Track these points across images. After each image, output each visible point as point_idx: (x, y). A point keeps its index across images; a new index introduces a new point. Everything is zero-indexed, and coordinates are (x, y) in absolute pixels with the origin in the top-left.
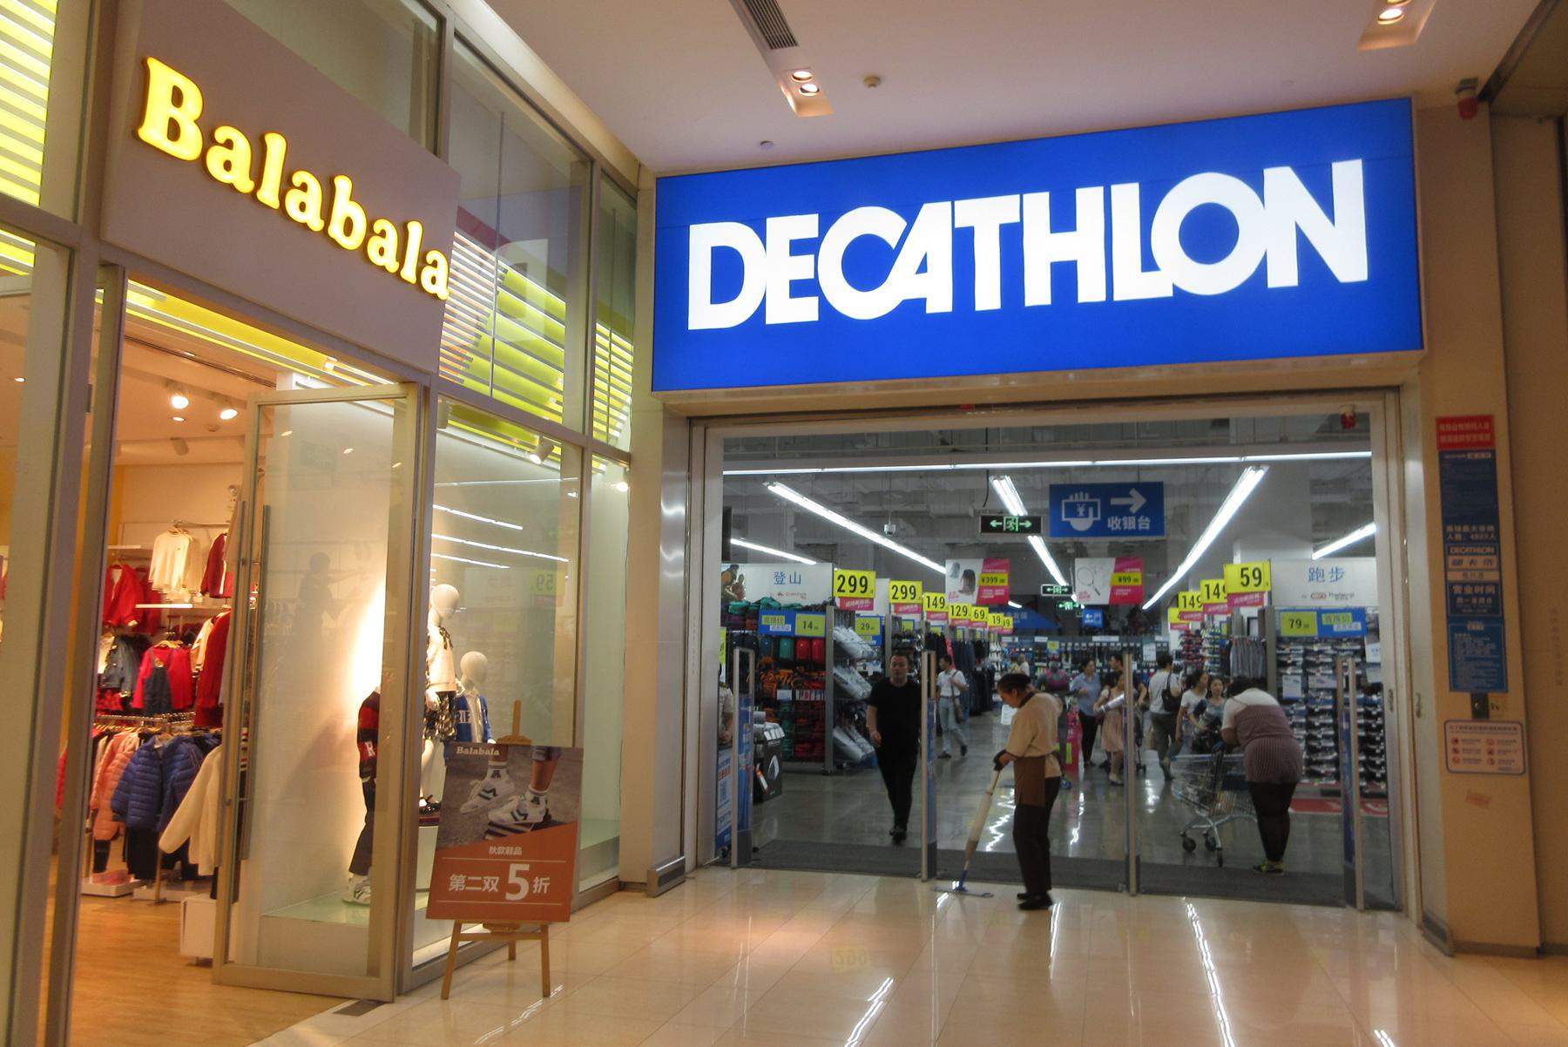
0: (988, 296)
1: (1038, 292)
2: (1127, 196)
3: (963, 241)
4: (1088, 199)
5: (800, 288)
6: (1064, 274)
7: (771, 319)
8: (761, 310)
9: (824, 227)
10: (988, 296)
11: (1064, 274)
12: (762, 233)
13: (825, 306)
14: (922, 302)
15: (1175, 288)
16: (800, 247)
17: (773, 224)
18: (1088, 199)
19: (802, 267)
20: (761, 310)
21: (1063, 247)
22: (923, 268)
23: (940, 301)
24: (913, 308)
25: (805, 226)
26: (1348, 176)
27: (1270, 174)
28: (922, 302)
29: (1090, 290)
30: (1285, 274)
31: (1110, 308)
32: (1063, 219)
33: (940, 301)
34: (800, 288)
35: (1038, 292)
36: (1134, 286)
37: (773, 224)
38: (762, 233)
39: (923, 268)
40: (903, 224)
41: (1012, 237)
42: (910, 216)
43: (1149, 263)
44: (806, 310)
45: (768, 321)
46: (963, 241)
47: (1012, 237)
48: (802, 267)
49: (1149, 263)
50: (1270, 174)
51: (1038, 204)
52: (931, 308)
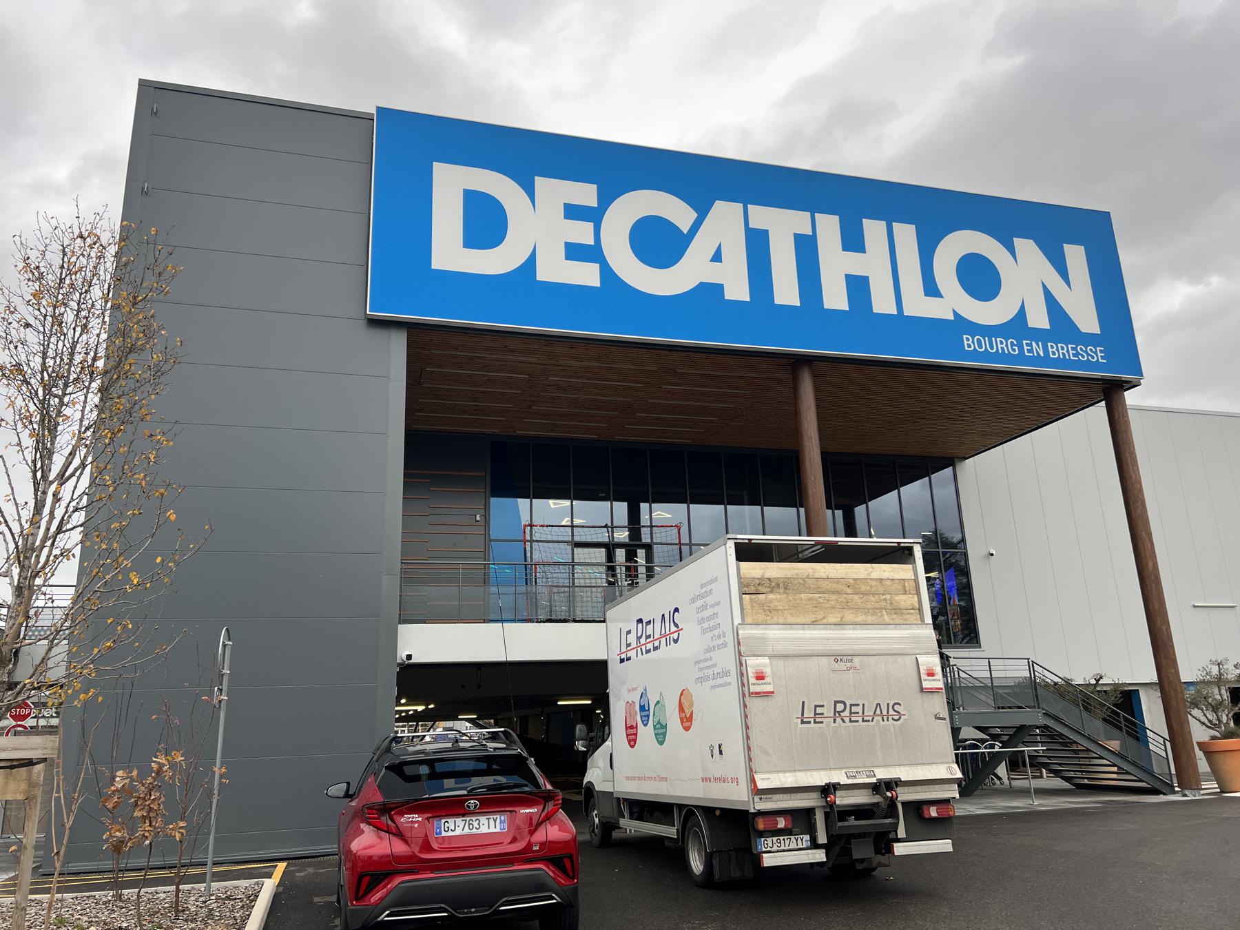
0: (786, 291)
1: (835, 298)
2: (906, 234)
3: (757, 243)
4: (873, 230)
5: (575, 252)
6: (858, 286)
7: (544, 273)
8: (530, 264)
9: (606, 199)
10: (786, 291)
11: (858, 286)
12: (530, 192)
13: (607, 272)
14: (719, 288)
15: (955, 313)
16: (573, 212)
17: (540, 182)
18: (873, 230)
19: (582, 233)
20: (532, 260)
21: (855, 264)
22: (717, 257)
23: (738, 289)
24: (709, 292)
25: (586, 194)
26: (1075, 255)
27: (1017, 242)
28: (719, 288)
29: (883, 303)
30: (1038, 319)
31: (901, 322)
32: (853, 241)
33: (738, 289)
34: (575, 252)
35: (835, 298)
36: (918, 305)
37: (540, 182)
38: (530, 192)
39: (717, 257)
40: (693, 215)
41: (806, 248)
42: (702, 211)
43: (931, 289)
44: (587, 275)
45: (544, 273)
46: (757, 243)
47: (806, 248)
48: (582, 233)
49: (931, 289)
50: (1017, 242)
51: (829, 227)
52: (729, 295)
